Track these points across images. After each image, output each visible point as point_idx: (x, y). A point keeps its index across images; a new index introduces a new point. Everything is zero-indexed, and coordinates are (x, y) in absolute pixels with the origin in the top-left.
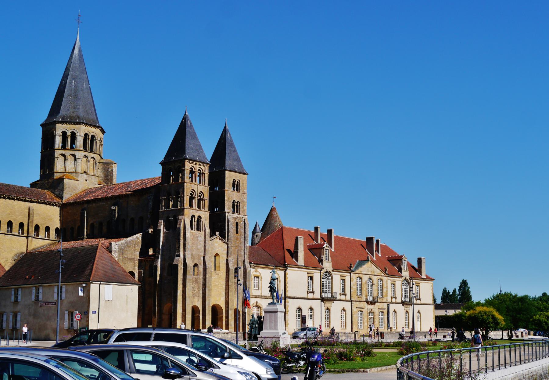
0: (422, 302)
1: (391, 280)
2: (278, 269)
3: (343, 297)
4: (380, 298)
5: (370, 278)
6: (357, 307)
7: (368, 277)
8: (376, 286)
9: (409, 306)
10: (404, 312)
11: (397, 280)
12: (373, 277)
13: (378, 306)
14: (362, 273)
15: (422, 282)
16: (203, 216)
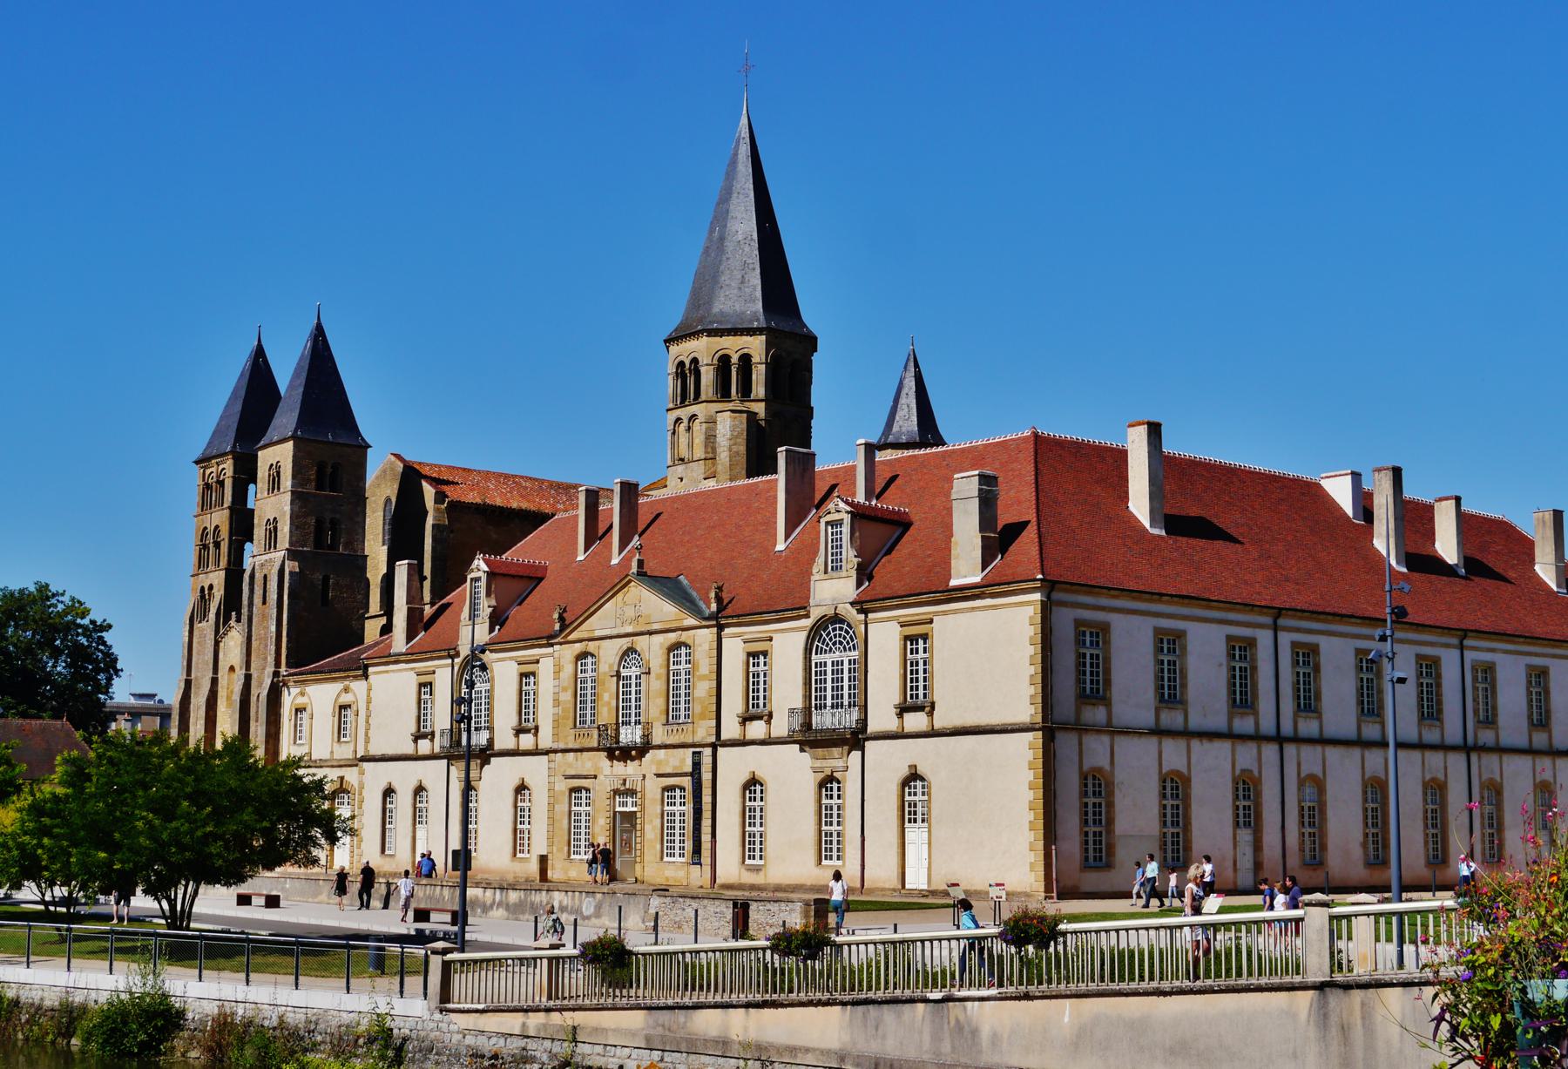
0: (940, 722)
1: (745, 637)
2: (349, 677)
3: (527, 741)
4: (675, 727)
5: (631, 650)
6: (567, 773)
7: (624, 643)
8: (658, 677)
9: (836, 751)
10: (810, 782)
11: (776, 631)
12: (641, 643)
13: (659, 763)
14: (598, 633)
15: (937, 613)
16: (215, 584)
